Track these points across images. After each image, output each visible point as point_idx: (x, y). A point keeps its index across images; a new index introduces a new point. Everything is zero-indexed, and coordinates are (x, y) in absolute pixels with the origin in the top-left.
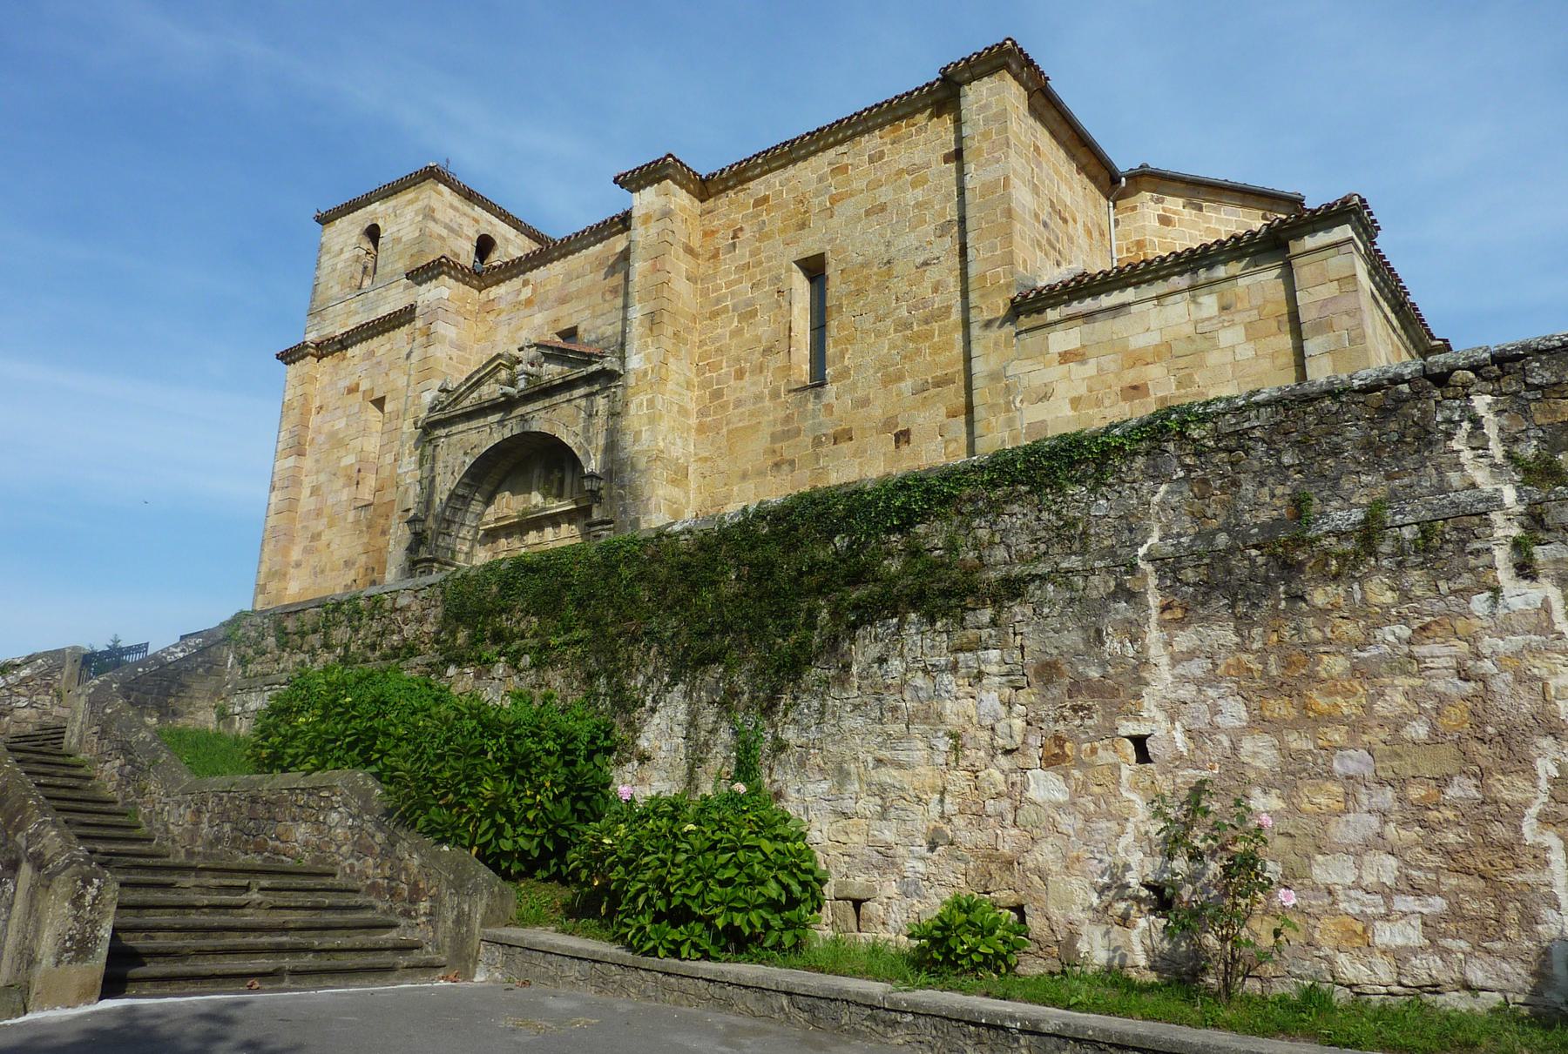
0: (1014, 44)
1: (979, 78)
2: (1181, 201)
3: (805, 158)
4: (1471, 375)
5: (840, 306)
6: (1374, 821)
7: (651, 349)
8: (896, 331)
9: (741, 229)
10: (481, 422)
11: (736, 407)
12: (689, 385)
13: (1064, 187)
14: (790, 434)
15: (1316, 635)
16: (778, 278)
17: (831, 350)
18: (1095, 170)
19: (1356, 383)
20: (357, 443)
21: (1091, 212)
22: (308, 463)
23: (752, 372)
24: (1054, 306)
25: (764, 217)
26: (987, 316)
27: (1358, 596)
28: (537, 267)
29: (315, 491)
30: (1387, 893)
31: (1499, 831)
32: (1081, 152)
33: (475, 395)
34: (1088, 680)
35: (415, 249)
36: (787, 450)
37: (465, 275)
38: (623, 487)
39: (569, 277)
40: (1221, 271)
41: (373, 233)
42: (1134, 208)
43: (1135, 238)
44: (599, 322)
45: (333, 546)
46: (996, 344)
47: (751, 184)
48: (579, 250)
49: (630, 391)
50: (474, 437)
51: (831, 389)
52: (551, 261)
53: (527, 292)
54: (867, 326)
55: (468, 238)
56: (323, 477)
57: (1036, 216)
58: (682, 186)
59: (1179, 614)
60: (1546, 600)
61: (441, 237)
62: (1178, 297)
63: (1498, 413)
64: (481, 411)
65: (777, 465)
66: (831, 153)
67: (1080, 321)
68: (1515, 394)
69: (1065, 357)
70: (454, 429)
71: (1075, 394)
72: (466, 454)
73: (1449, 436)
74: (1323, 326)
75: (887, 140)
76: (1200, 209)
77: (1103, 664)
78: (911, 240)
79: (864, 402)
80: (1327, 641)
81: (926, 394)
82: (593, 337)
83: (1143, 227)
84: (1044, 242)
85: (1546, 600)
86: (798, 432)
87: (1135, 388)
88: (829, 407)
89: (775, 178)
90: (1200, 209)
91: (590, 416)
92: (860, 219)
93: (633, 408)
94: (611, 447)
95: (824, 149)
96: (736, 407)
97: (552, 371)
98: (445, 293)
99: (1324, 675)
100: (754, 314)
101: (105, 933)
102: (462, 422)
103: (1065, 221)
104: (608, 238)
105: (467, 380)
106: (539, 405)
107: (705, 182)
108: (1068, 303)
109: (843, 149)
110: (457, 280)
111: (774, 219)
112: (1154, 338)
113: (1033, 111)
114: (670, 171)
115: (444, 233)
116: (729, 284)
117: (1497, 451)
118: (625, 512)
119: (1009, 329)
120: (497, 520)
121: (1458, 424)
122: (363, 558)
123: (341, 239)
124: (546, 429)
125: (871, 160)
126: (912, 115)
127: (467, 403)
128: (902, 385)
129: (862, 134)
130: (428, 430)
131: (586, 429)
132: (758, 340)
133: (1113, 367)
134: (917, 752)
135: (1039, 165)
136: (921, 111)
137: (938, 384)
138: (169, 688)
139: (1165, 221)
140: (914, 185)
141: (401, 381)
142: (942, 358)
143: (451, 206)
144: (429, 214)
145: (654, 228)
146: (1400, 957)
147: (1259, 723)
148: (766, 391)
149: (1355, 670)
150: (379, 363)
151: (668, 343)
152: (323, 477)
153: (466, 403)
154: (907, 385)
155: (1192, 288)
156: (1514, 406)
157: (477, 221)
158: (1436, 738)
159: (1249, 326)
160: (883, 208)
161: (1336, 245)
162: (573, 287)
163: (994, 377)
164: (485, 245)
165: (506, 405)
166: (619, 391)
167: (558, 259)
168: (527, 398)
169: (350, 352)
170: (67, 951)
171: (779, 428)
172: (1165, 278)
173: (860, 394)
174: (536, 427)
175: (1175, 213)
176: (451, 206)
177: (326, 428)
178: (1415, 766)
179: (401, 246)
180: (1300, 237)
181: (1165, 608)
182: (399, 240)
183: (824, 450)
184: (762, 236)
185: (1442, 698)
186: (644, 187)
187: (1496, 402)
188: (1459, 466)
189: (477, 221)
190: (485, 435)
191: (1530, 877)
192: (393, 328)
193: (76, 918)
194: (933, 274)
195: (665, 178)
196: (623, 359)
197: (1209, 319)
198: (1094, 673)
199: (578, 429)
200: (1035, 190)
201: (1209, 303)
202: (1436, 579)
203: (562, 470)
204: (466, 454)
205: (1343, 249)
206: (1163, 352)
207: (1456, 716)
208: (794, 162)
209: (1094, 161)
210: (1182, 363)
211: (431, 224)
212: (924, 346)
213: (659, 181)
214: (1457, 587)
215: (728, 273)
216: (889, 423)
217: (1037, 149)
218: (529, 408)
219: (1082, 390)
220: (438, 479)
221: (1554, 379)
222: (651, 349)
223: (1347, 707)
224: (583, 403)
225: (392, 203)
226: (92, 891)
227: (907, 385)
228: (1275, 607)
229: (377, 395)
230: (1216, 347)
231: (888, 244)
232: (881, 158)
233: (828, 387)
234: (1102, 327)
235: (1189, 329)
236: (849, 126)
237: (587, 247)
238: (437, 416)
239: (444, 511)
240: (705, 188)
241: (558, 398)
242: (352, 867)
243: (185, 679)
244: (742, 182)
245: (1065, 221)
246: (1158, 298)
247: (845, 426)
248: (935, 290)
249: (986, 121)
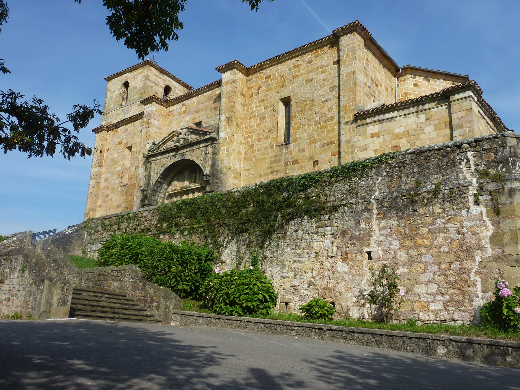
0: (359, 22)
1: (347, 34)
2: (422, 78)
3: (284, 62)
4: (468, 146)
5: (295, 116)
6: (432, 275)
7: (228, 130)
8: (315, 125)
9: (261, 87)
10: (167, 155)
11: (258, 151)
12: (241, 143)
13: (377, 73)
14: (277, 161)
15: (420, 222)
16: (274, 105)
17: (292, 131)
18: (390, 67)
19: (436, 147)
20: (121, 163)
21: (388, 82)
22: (104, 169)
23: (264, 139)
24: (370, 117)
25: (269, 83)
26: (346, 120)
27: (431, 210)
28: (188, 99)
29: (106, 180)
30: (434, 295)
31: (465, 277)
32: (385, 61)
33: (165, 146)
34: (355, 235)
35: (142, 91)
36: (276, 167)
37: (161, 102)
38: (217, 179)
39: (199, 103)
40: (427, 106)
41: (126, 85)
42: (404, 80)
43: (404, 92)
44: (209, 120)
45: (113, 200)
46: (349, 130)
47: (265, 71)
48: (203, 93)
49: (220, 145)
50: (164, 161)
51: (291, 145)
52: (193, 97)
53: (184, 108)
54: (305, 123)
55: (161, 87)
56: (109, 175)
57: (366, 84)
58: (240, 71)
59: (382, 216)
60: (481, 211)
61: (152, 87)
62: (412, 115)
63: (474, 157)
64: (167, 152)
65: (272, 172)
66: (294, 60)
67: (378, 123)
68: (479, 151)
69: (373, 135)
70: (158, 158)
71: (376, 149)
72: (162, 167)
73: (460, 164)
74: (460, 126)
75: (313, 56)
76: (429, 81)
77: (360, 231)
78: (321, 92)
79: (303, 150)
80: (422, 223)
81: (324, 148)
82: (207, 125)
83: (408, 88)
84: (368, 94)
85: (481, 211)
86: (280, 161)
88: (291, 152)
89: (273, 69)
90: (429, 81)
91: (206, 154)
92: (303, 84)
93: (221, 151)
94: (214, 165)
95: (291, 59)
96: (258, 151)
97: (193, 138)
98: (154, 108)
99: (421, 233)
100: (265, 118)
101: (70, 299)
102: (160, 155)
103: (377, 86)
104: (213, 89)
105: (162, 140)
106: (188, 150)
107: (248, 69)
108: (374, 116)
109: (297, 59)
110: (159, 104)
111: (273, 83)
112: (403, 129)
113: (366, 46)
114: (236, 66)
115: (153, 85)
116: (256, 107)
117: (473, 168)
118: (218, 188)
119: (354, 125)
120: (173, 191)
121: (463, 160)
122: (124, 204)
123: (114, 87)
124: (190, 158)
125: (308, 63)
126: (323, 47)
127: (162, 149)
128: (316, 144)
129: (305, 53)
130: (148, 158)
131: (205, 159)
132: (266, 127)
133: (389, 139)
134: (306, 258)
135: (368, 65)
136: (326, 45)
137: (329, 144)
138: (66, 243)
139: (416, 85)
140: (322, 72)
141: (138, 140)
142: (330, 135)
143: (155, 75)
144: (147, 78)
145: (230, 86)
146: (436, 312)
147: (403, 247)
148: (269, 146)
149: (430, 232)
150: (130, 134)
151: (234, 128)
152: (109, 175)
153: (162, 149)
154: (318, 144)
155: (417, 112)
156: (479, 155)
157: (164, 80)
158: (450, 251)
159: (435, 126)
160: (311, 80)
161: (466, 98)
162: (200, 107)
163: (348, 142)
164: (167, 90)
165: (176, 149)
166: (217, 145)
167: (195, 96)
168: (184, 147)
169: (119, 129)
170: (60, 303)
171: (273, 159)
172: (408, 108)
173: (301, 147)
174: (187, 157)
175: (420, 82)
176: (155, 75)
177: (110, 157)
178: (444, 259)
179: (137, 90)
180: (454, 95)
181: (378, 214)
182: (136, 87)
183: (289, 167)
184: (268, 89)
185: (452, 240)
186: (227, 71)
187: (474, 154)
188: (462, 172)
189: (164, 80)
190: (169, 160)
191: (472, 289)
192: (135, 121)
193: (62, 294)
194: (328, 105)
195: (234, 68)
196: (218, 134)
197: (422, 123)
198: (357, 234)
199: (202, 158)
200: (366, 75)
201: (422, 117)
202: (453, 205)
203: (196, 173)
204: (162, 167)
205: (468, 99)
206: (406, 134)
207: (455, 244)
208: (281, 63)
209: (389, 63)
210: (412, 138)
211: (148, 82)
212: (325, 130)
213: (232, 69)
214: (458, 207)
215: (256, 103)
216: (311, 158)
217: (367, 60)
218: (184, 151)
219: (378, 147)
220: (152, 176)
221: (490, 147)
222: (228, 130)
223: (427, 242)
224: (204, 149)
225: (133, 73)
226: (66, 287)
227: (318, 144)
228: (409, 213)
229: (129, 145)
230: (424, 133)
231: (313, 94)
232: (311, 62)
233: (290, 145)
234: (386, 125)
235: (415, 126)
236: (300, 50)
237: (206, 92)
238: (151, 153)
239: (154, 187)
240: (248, 72)
241: (195, 147)
242: (132, 294)
243: (71, 240)
244: (262, 70)
245: (377, 86)
246: (405, 115)
247: (296, 158)
248: (329, 110)
249: (348, 50)
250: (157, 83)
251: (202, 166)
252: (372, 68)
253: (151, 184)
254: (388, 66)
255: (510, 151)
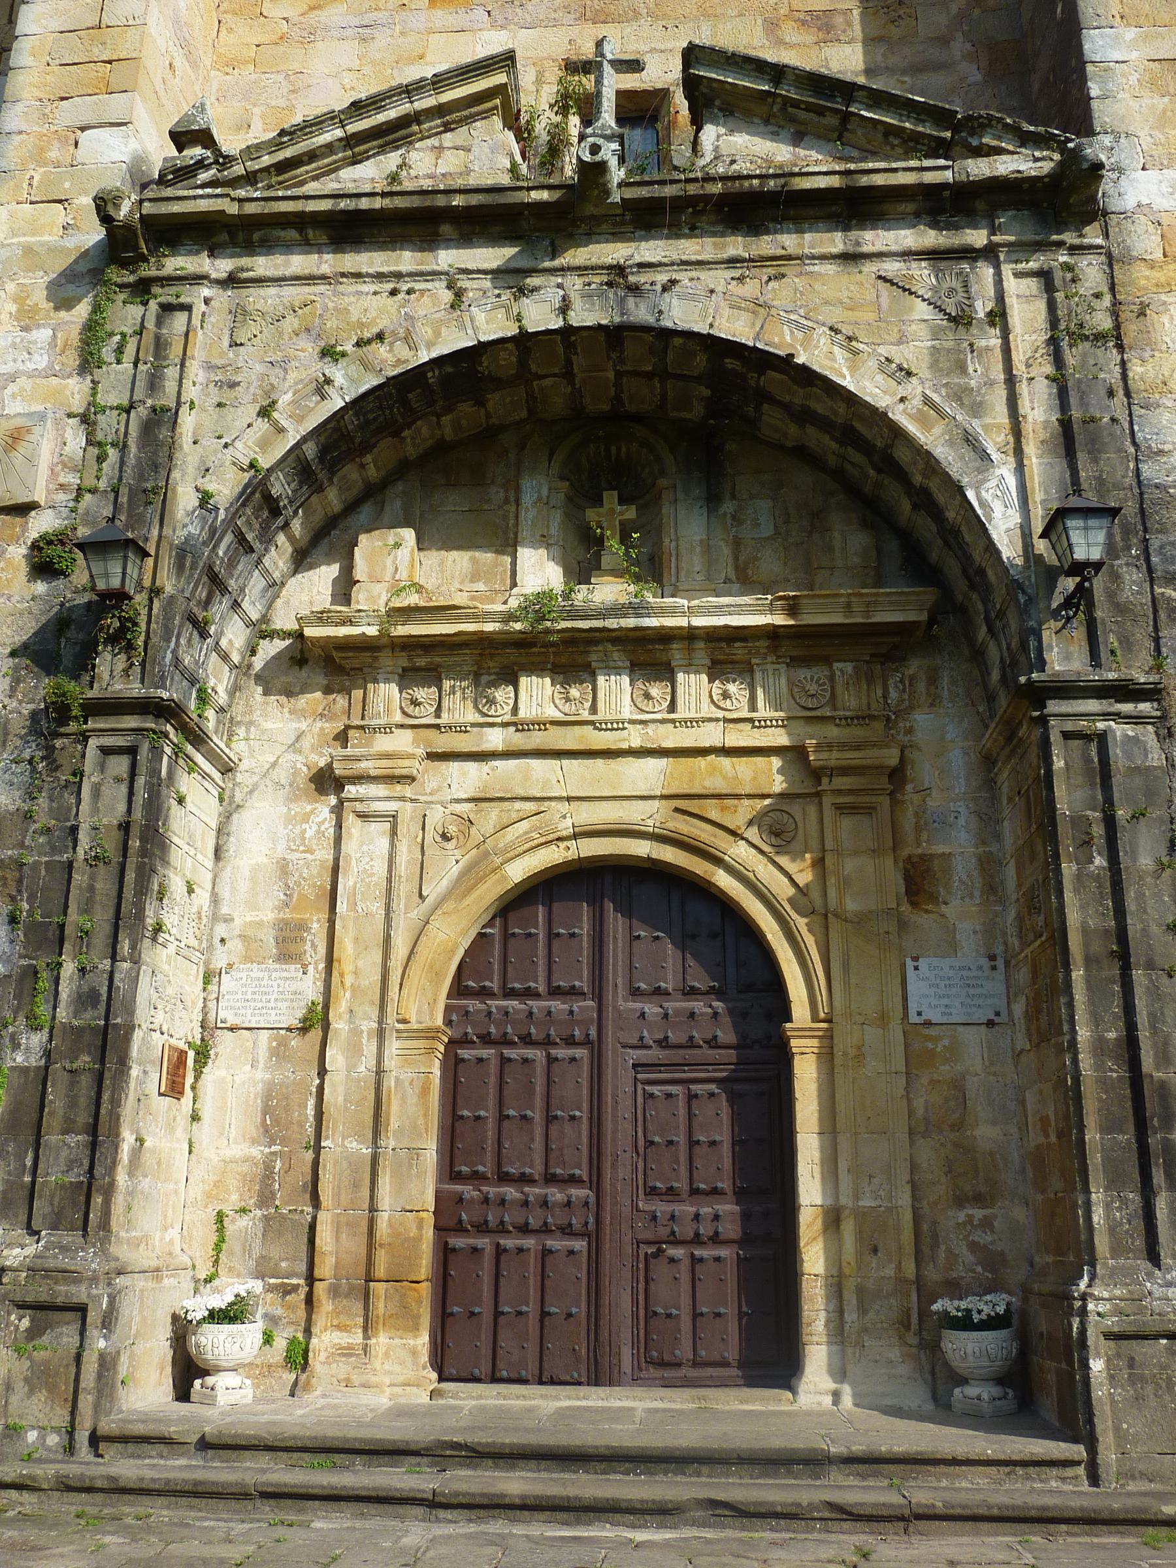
10: (407, 260)
33: (392, 160)
50: (369, 306)
64: (421, 221)
70: (262, 265)
102: (307, 245)
105: (358, 108)
106: (690, 248)
127: (320, 190)
166: (1091, 271)
190: (443, 309)
199: (915, 352)
204: (329, 353)
218: (651, 250)
251: (920, 418)
253: (185, 499)
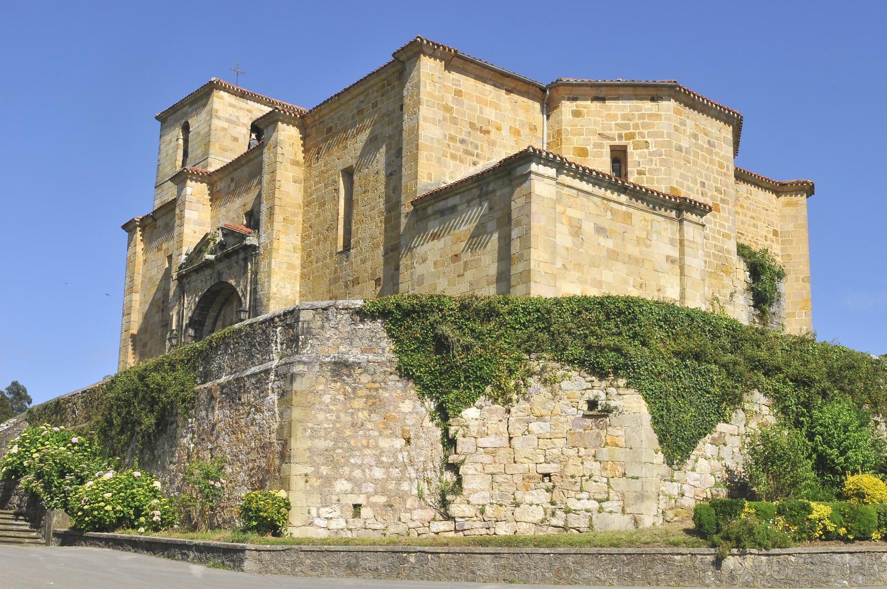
32: (507, 81)
55: (244, 125)
57: (452, 138)
61: (224, 129)
79: (363, 261)
87: (456, 255)
94: (254, 291)
115: (226, 125)
139: (577, 114)
143: (231, 105)
159: (498, 220)
171: (332, 276)
176: (231, 105)
189: (250, 111)
190: (202, 284)
209: (520, 83)
217: (459, 93)
250: (234, 119)
252: (474, 103)
254: (518, 88)
255: (303, 327)
